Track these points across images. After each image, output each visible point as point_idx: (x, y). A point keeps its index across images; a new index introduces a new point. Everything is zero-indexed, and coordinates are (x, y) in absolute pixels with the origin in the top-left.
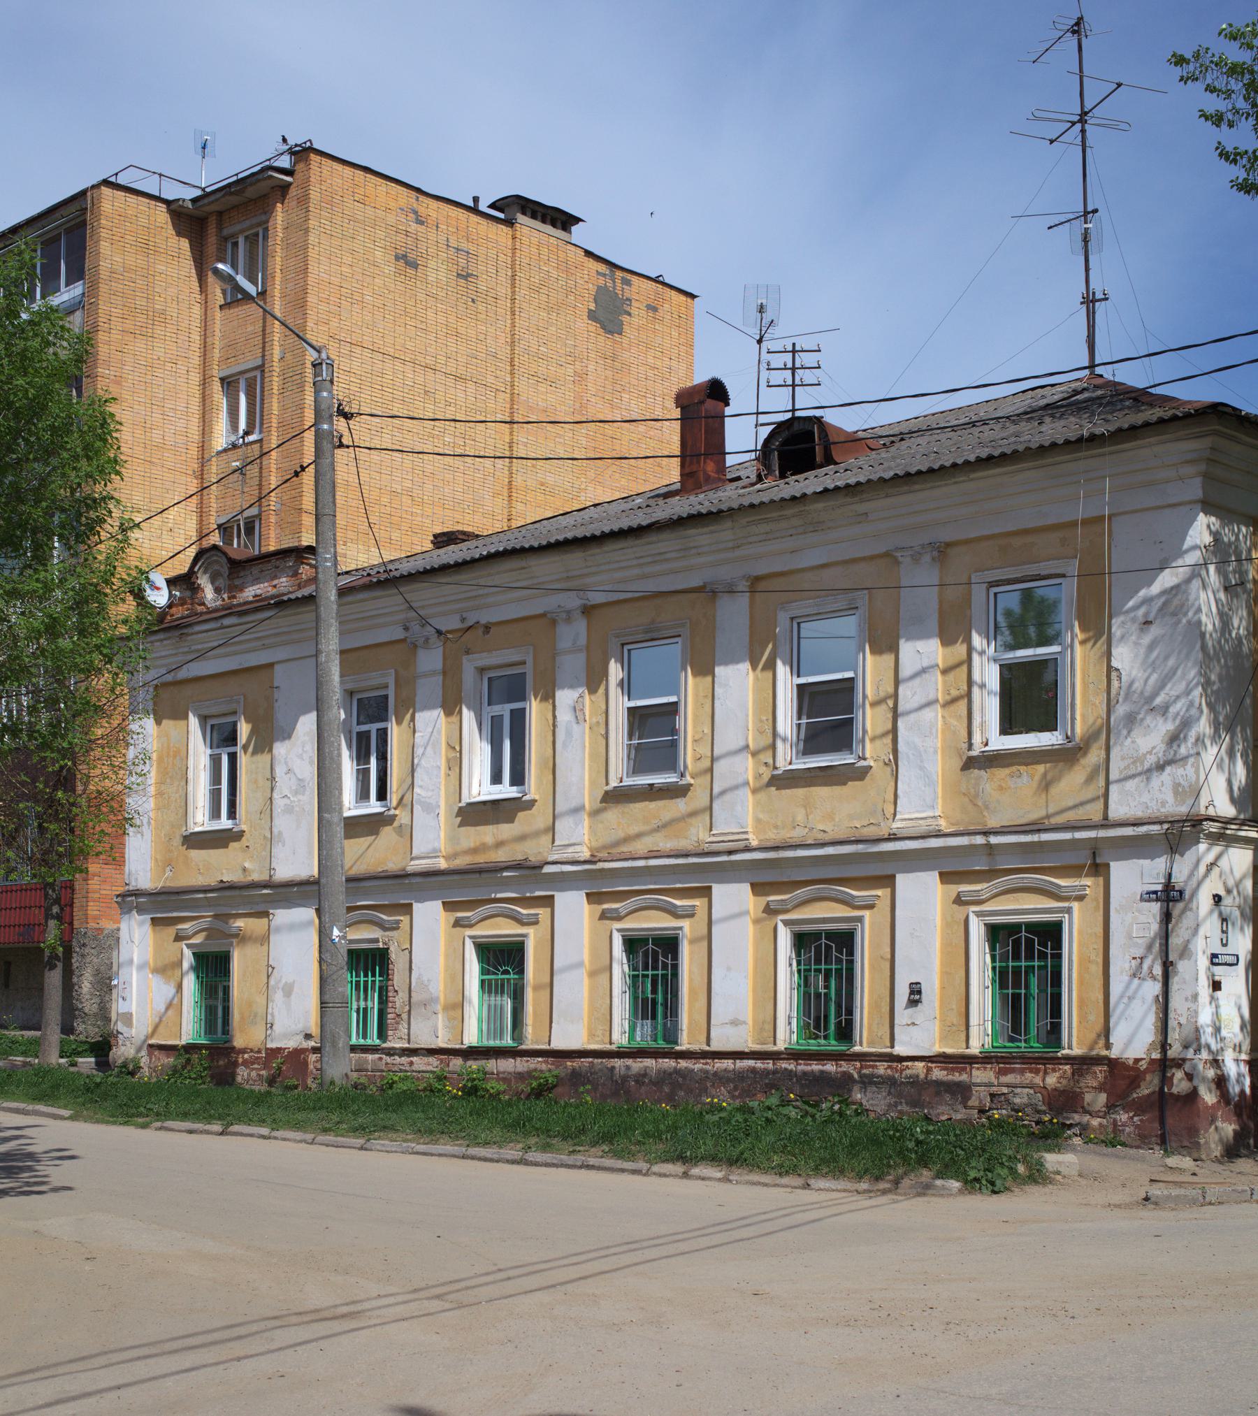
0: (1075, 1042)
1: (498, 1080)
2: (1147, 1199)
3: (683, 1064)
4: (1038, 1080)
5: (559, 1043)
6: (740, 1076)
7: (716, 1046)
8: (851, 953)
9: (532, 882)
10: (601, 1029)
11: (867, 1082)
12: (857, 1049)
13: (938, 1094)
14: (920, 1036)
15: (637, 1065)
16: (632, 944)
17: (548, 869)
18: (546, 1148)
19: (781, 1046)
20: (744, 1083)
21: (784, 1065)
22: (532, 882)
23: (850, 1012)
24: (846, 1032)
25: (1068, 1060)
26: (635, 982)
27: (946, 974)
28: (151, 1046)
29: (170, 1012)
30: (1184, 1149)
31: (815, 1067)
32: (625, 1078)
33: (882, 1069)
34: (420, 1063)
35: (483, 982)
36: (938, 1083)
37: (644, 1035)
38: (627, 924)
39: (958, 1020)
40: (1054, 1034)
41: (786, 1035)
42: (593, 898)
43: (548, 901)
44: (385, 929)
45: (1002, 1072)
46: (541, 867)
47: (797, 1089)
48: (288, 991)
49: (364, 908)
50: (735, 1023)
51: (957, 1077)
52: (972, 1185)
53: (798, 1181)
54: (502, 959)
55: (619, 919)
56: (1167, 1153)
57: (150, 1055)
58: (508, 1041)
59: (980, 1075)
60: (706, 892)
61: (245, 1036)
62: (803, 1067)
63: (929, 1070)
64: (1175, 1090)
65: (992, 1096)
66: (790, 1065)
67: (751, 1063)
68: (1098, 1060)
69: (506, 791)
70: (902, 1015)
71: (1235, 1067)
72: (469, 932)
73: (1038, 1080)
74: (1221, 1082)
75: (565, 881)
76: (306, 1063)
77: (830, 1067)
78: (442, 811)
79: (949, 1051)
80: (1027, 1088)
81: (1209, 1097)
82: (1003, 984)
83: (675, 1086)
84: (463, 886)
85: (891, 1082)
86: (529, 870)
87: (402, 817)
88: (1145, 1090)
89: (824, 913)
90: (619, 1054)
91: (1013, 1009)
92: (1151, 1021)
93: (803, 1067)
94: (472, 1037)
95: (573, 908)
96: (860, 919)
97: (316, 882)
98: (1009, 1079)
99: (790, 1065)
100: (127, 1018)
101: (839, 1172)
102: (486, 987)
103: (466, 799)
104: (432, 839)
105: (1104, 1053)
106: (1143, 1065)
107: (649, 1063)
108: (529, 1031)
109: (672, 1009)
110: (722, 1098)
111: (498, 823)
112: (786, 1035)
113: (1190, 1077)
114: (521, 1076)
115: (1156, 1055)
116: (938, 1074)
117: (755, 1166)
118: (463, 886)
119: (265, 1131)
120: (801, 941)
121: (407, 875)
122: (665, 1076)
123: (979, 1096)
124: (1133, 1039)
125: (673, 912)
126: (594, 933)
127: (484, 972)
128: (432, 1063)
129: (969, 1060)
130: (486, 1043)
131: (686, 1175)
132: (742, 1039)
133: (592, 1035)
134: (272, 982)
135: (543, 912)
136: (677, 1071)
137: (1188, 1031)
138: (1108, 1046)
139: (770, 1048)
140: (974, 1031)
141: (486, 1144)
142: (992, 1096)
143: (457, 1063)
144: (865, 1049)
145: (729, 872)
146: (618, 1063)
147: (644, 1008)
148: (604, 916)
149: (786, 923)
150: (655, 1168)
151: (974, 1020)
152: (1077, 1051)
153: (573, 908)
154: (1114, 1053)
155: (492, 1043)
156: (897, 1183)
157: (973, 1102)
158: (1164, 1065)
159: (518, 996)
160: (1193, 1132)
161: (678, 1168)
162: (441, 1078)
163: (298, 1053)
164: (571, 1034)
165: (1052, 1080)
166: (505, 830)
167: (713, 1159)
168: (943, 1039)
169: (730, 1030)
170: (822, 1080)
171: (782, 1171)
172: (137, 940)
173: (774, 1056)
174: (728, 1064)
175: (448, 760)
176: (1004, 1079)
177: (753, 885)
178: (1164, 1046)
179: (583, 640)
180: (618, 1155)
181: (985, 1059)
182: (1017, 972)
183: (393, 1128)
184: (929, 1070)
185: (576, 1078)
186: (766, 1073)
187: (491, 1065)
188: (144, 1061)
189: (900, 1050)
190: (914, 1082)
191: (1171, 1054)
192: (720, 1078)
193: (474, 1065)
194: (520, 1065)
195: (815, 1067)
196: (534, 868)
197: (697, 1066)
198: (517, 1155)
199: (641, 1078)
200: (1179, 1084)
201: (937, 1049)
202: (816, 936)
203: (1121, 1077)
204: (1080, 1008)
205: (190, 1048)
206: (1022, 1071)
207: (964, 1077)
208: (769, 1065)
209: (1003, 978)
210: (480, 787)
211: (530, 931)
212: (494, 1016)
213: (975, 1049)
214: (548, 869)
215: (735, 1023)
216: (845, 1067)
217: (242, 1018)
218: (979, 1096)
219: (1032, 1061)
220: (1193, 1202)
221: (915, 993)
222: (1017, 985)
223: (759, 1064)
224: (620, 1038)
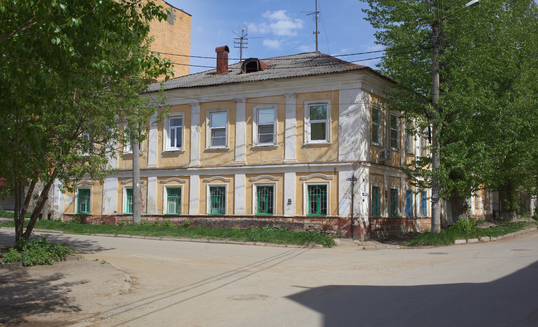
0: (330, 213)
1: (174, 223)
2: (364, 248)
3: (227, 219)
4: (321, 222)
5: (191, 214)
6: (242, 222)
7: (236, 214)
8: (272, 191)
9: (184, 172)
10: (204, 210)
11: (277, 223)
12: (274, 215)
13: (295, 226)
14: (291, 212)
15: (214, 219)
16: (212, 189)
17: (188, 169)
18: (213, 239)
19: (254, 214)
20: (243, 224)
21: (255, 219)
22: (184, 172)
23: (272, 206)
24: (271, 211)
25: (328, 218)
26: (212, 198)
27: (297, 197)
28: (64, 215)
29: (71, 206)
30: (357, 239)
31: (263, 220)
32: (210, 223)
33: (281, 220)
34: (150, 219)
35: (168, 198)
36: (296, 223)
37: (215, 212)
38: (211, 183)
39: (300, 208)
40: (324, 212)
41: (255, 212)
42: (201, 177)
43: (189, 177)
44: (181, 183)
45: (311, 221)
46: (187, 168)
47: (258, 225)
48: (109, 200)
49: (174, 178)
50: (241, 209)
51: (300, 222)
52: (325, 246)
53: (284, 246)
54: (174, 192)
55: (209, 182)
56: (353, 240)
57: (64, 217)
58: (175, 213)
59: (306, 221)
60: (233, 176)
61: (94, 211)
62: (260, 220)
63: (293, 220)
64: (355, 224)
65: (309, 226)
66: (256, 219)
67: (245, 219)
68: (336, 218)
69: (175, 148)
70: (286, 207)
71: (366, 219)
72: (165, 185)
73: (321, 222)
74: (364, 223)
75: (194, 172)
76: (115, 219)
77: (267, 220)
78: (157, 153)
79: (298, 215)
80: (318, 224)
81: (362, 226)
82: (312, 200)
83: (225, 224)
84: (162, 174)
85: (283, 223)
86: (182, 168)
87: (145, 154)
88: (347, 224)
89: (264, 182)
90: (209, 217)
91: (313, 206)
92: (349, 208)
93: (260, 220)
94: (165, 212)
95: (195, 180)
96: (275, 183)
97: (132, 170)
98: (314, 222)
99: (256, 219)
100: (57, 207)
101: (293, 243)
102: (169, 199)
103: (164, 150)
104: (155, 161)
105: (337, 216)
106: (347, 219)
107: (217, 219)
108: (182, 211)
109: (271, 204)
110: (237, 227)
111: (173, 157)
112: (255, 212)
113: (359, 222)
114: (180, 222)
115: (350, 217)
116: (295, 221)
117: (272, 242)
118: (162, 174)
119: (129, 236)
120: (259, 188)
121: (147, 170)
122: (221, 222)
123: (306, 227)
124: (344, 213)
125: (224, 181)
126: (201, 185)
127: (169, 195)
128: (154, 219)
129: (304, 218)
130: (168, 213)
131: (255, 244)
132: (243, 213)
133: (201, 212)
134: (104, 197)
135: (187, 180)
136: (225, 221)
137: (358, 212)
138: (338, 214)
139: (251, 215)
140: (305, 211)
141: (196, 238)
142: (309, 226)
143: (161, 219)
144: (276, 215)
145: (240, 171)
146: (208, 219)
147: (214, 205)
148: (204, 181)
149: (255, 184)
150: (246, 243)
151: (305, 208)
152: (330, 216)
153: (195, 180)
154: (340, 216)
155: (170, 214)
156: (307, 245)
157: (305, 228)
158: (352, 219)
159: (179, 201)
160: (359, 234)
161: (253, 243)
162: (156, 223)
163: (112, 216)
164: (195, 211)
165: (324, 223)
166: (175, 159)
167: (261, 241)
168: (297, 213)
169: (240, 211)
170: (265, 223)
171: (279, 243)
172: (112, 185)
173: (252, 217)
174: (239, 219)
175: (159, 140)
176: (312, 222)
177: (246, 175)
178: (352, 214)
179: (199, 111)
180: (234, 240)
181: (308, 218)
182: (315, 197)
183: (165, 235)
184: (293, 220)
185: (196, 223)
186: (250, 221)
187: (171, 219)
188: (62, 219)
189: (285, 215)
190: (289, 223)
191: (354, 216)
192: (237, 222)
193: (167, 219)
194: (180, 219)
195: (263, 220)
196: (185, 168)
197: (231, 219)
198: (207, 241)
199: (215, 223)
200: (356, 223)
201: (295, 215)
202: (315, 186)
203: (341, 221)
204: (331, 205)
205: (76, 215)
206: (317, 221)
207: (302, 222)
208: (251, 219)
209: (311, 198)
210: (168, 147)
211: (183, 185)
212: (171, 207)
213: (305, 215)
214: (188, 169)
215: (241, 209)
216: (271, 219)
217: (94, 207)
218: (306, 227)
219: (319, 218)
220: (374, 249)
221: (290, 201)
222: (315, 200)
223: (248, 219)
224: (209, 212)
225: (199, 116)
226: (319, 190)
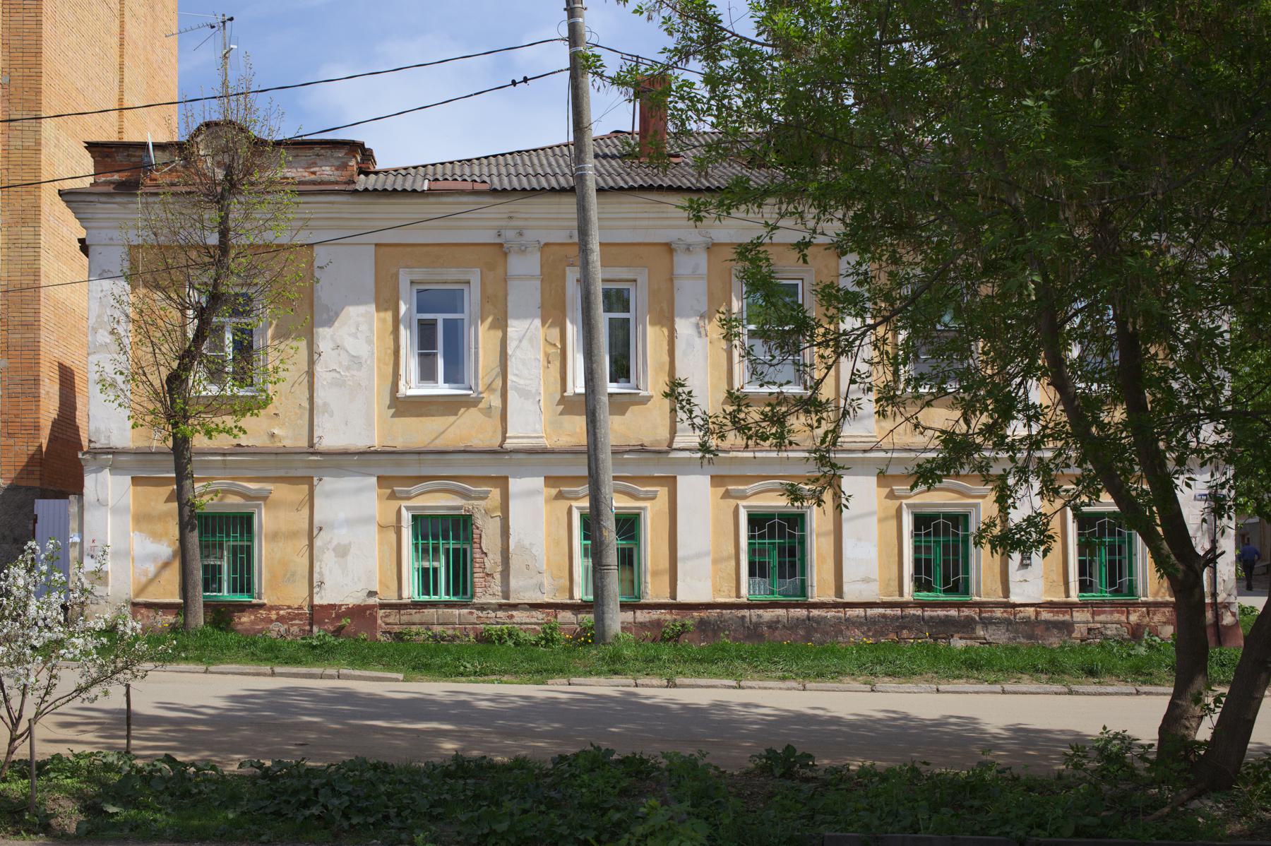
4: (1123, 618)
5: (682, 597)
6: (868, 623)
7: (848, 598)
11: (986, 623)
12: (977, 599)
13: (1047, 629)
15: (768, 615)
21: (912, 611)
25: (1145, 604)
28: (134, 605)
31: (941, 613)
33: (999, 613)
34: (519, 616)
36: (1047, 622)
48: (342, 552)
50: (866, 580)
51: (1061, 618)
55: (745, 497)
59: (1080, 616)
62: (929, 613)
63: (1037, 613)
64: (1225, 622)
65: (1090, 630)
66: (919, 612)
67: (881, 611)
79: (1055, 599)
85: (1008, 622)
90: (749, 606)
93: (929, 613)
98: (1102, 618)
99: (919, 612)
107: (781, 612)
116: (1046, 615)
123: (1080, 631)
128: (539, 616)
133: (717, 590)
139: (896, 598)
142: (1090, 630)
146: (746, 612)
148: (727, 495)
152: (1150, 599)
164: (697, 586)
165: (1134, 618)
168: (1047, 591)
174: (860, 612)
175: (547, 356)
176: (1097, 618)
179: (703, 268)
186: (895, 618)
189: (1014, 599)
190: (1027, 622)
191: (1219, 600)
192: (850, 622)
195: (941, 613)
197: (831, 614)
199: (773, 625)
206: (1111, 613)
207: (1067, 617)
208: (898, 612)
214: (673, 455)
215: (866, 580)
216: (966, 612)
218: (1080, 631)
223: (889, 612)
225: (702, 286)
226: (781, 527)
